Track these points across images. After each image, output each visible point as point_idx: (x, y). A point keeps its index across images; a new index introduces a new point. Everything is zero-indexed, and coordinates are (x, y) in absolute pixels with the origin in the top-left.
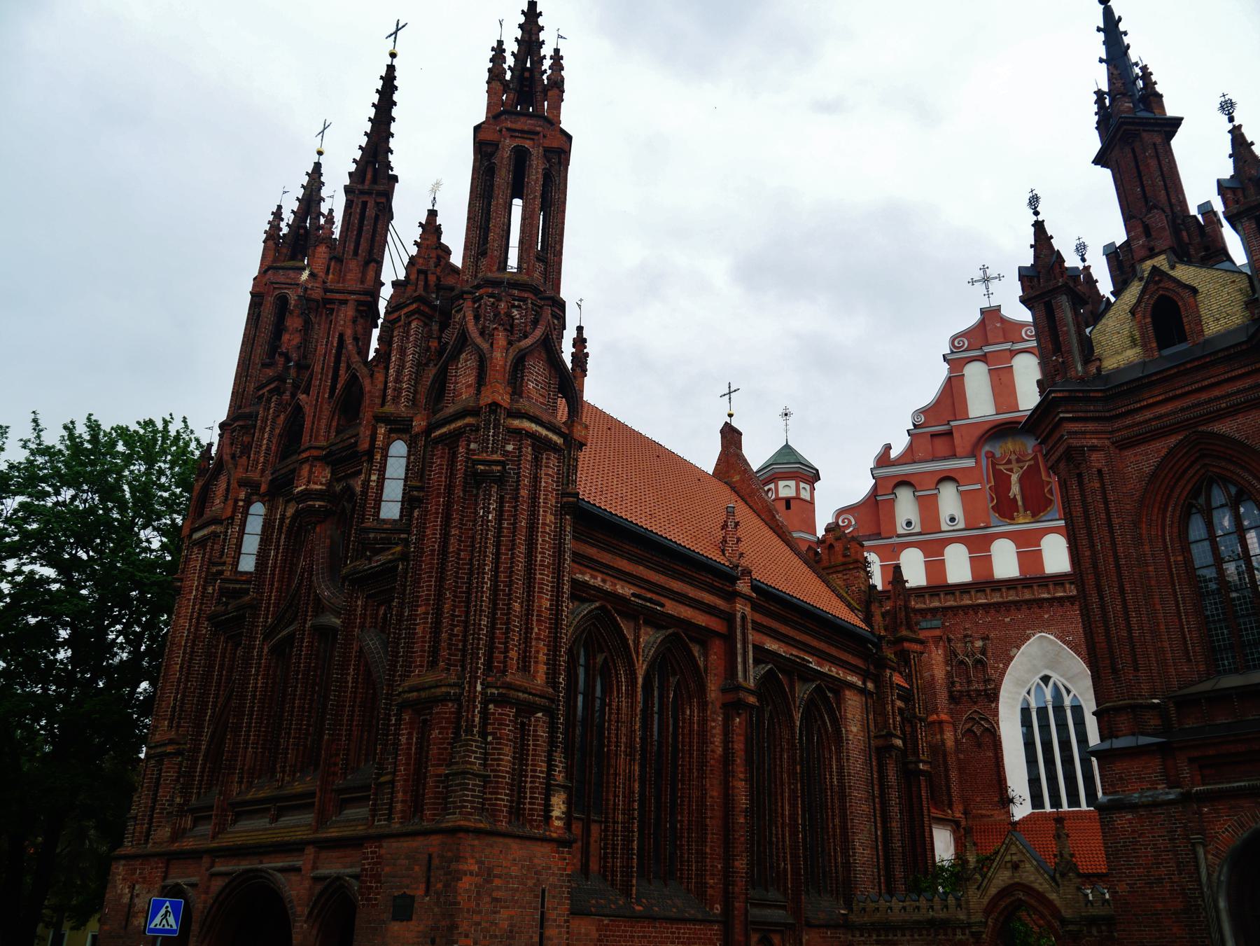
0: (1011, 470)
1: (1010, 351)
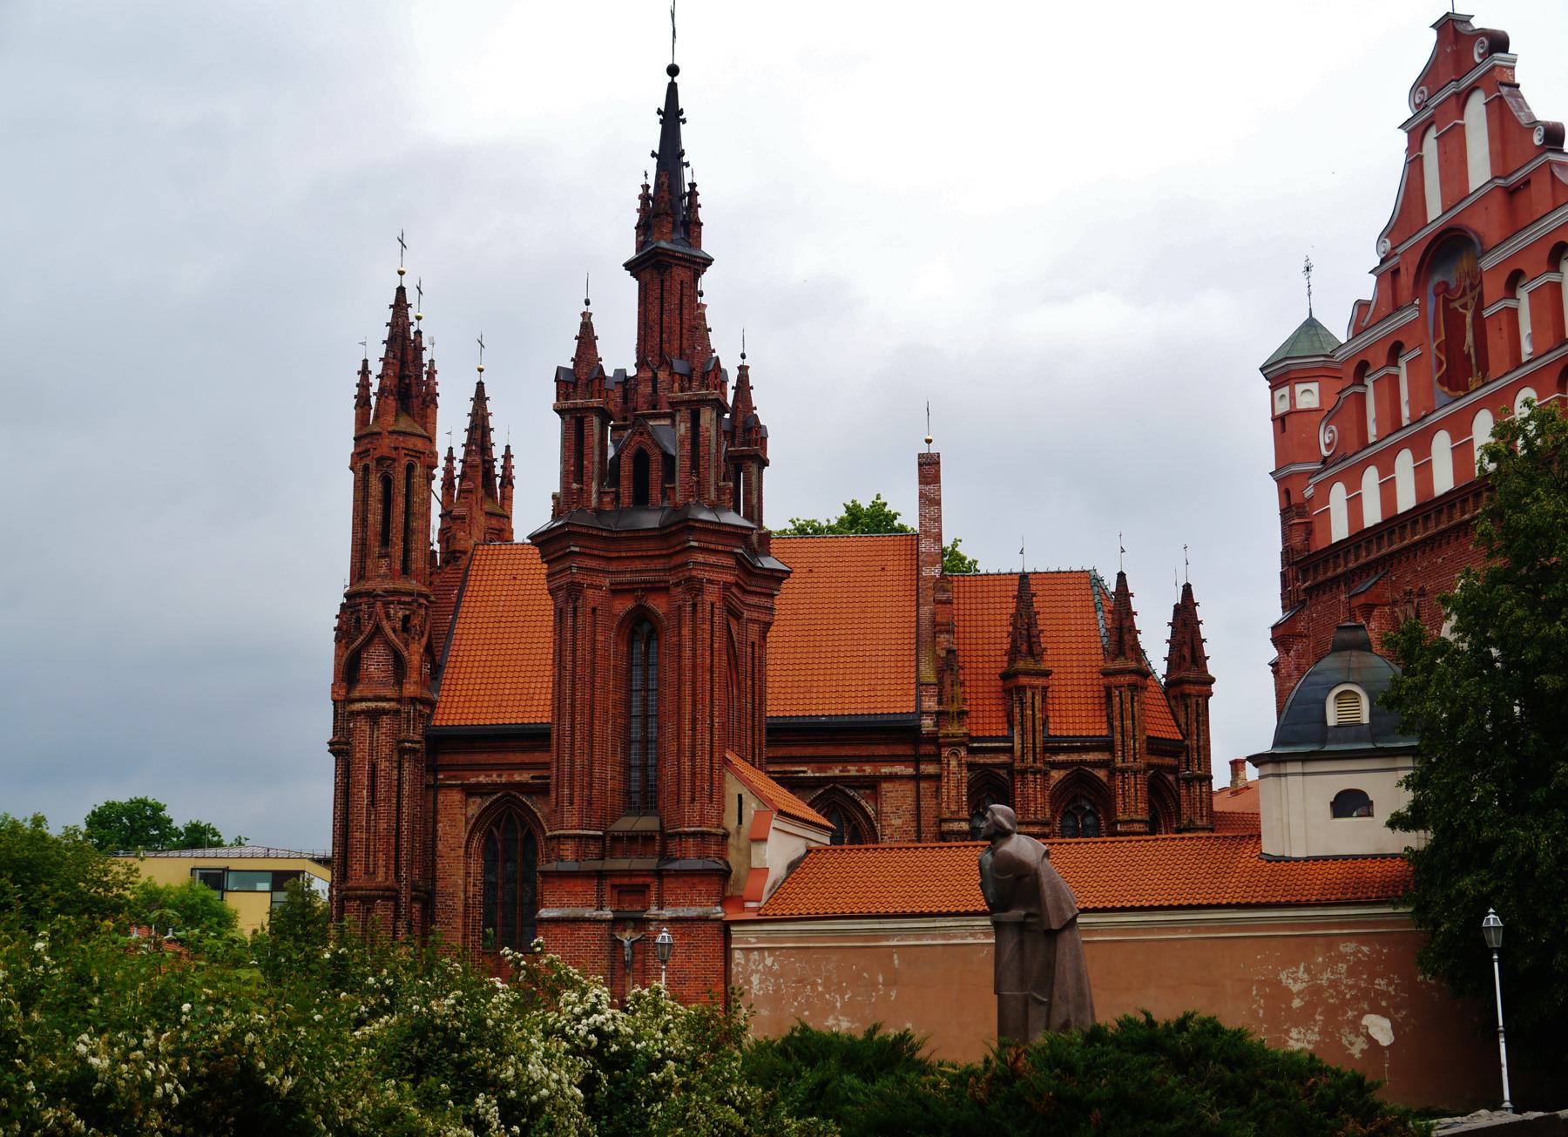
0: (1464, 306)
1: (1456, 94)
